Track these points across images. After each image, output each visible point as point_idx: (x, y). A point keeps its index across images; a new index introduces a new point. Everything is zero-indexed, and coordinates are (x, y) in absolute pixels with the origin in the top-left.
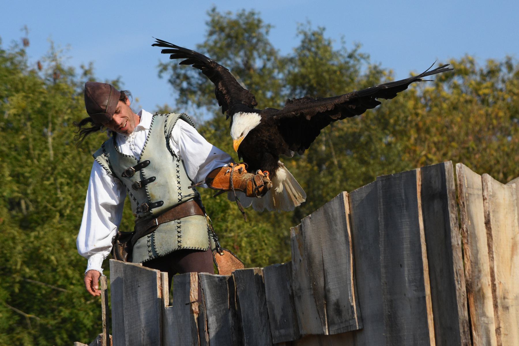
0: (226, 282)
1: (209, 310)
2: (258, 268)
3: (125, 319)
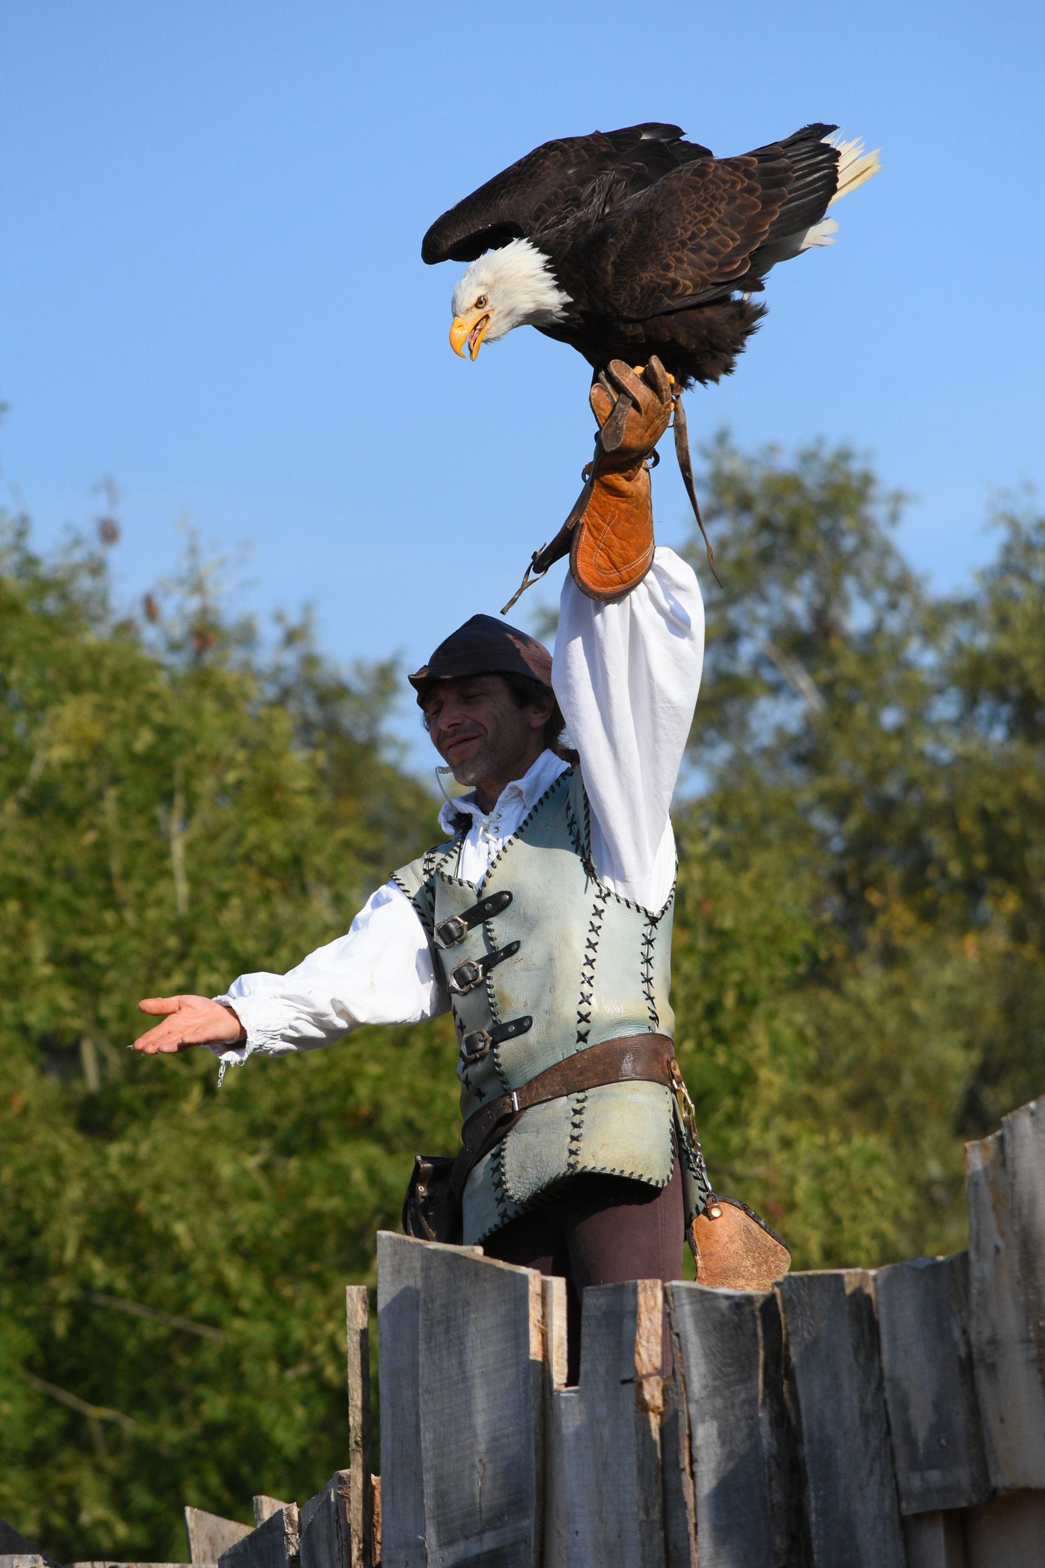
0: (752, 1313)
1: (697, 1402)
2: (859, 1270)
3: (422, 1425)
